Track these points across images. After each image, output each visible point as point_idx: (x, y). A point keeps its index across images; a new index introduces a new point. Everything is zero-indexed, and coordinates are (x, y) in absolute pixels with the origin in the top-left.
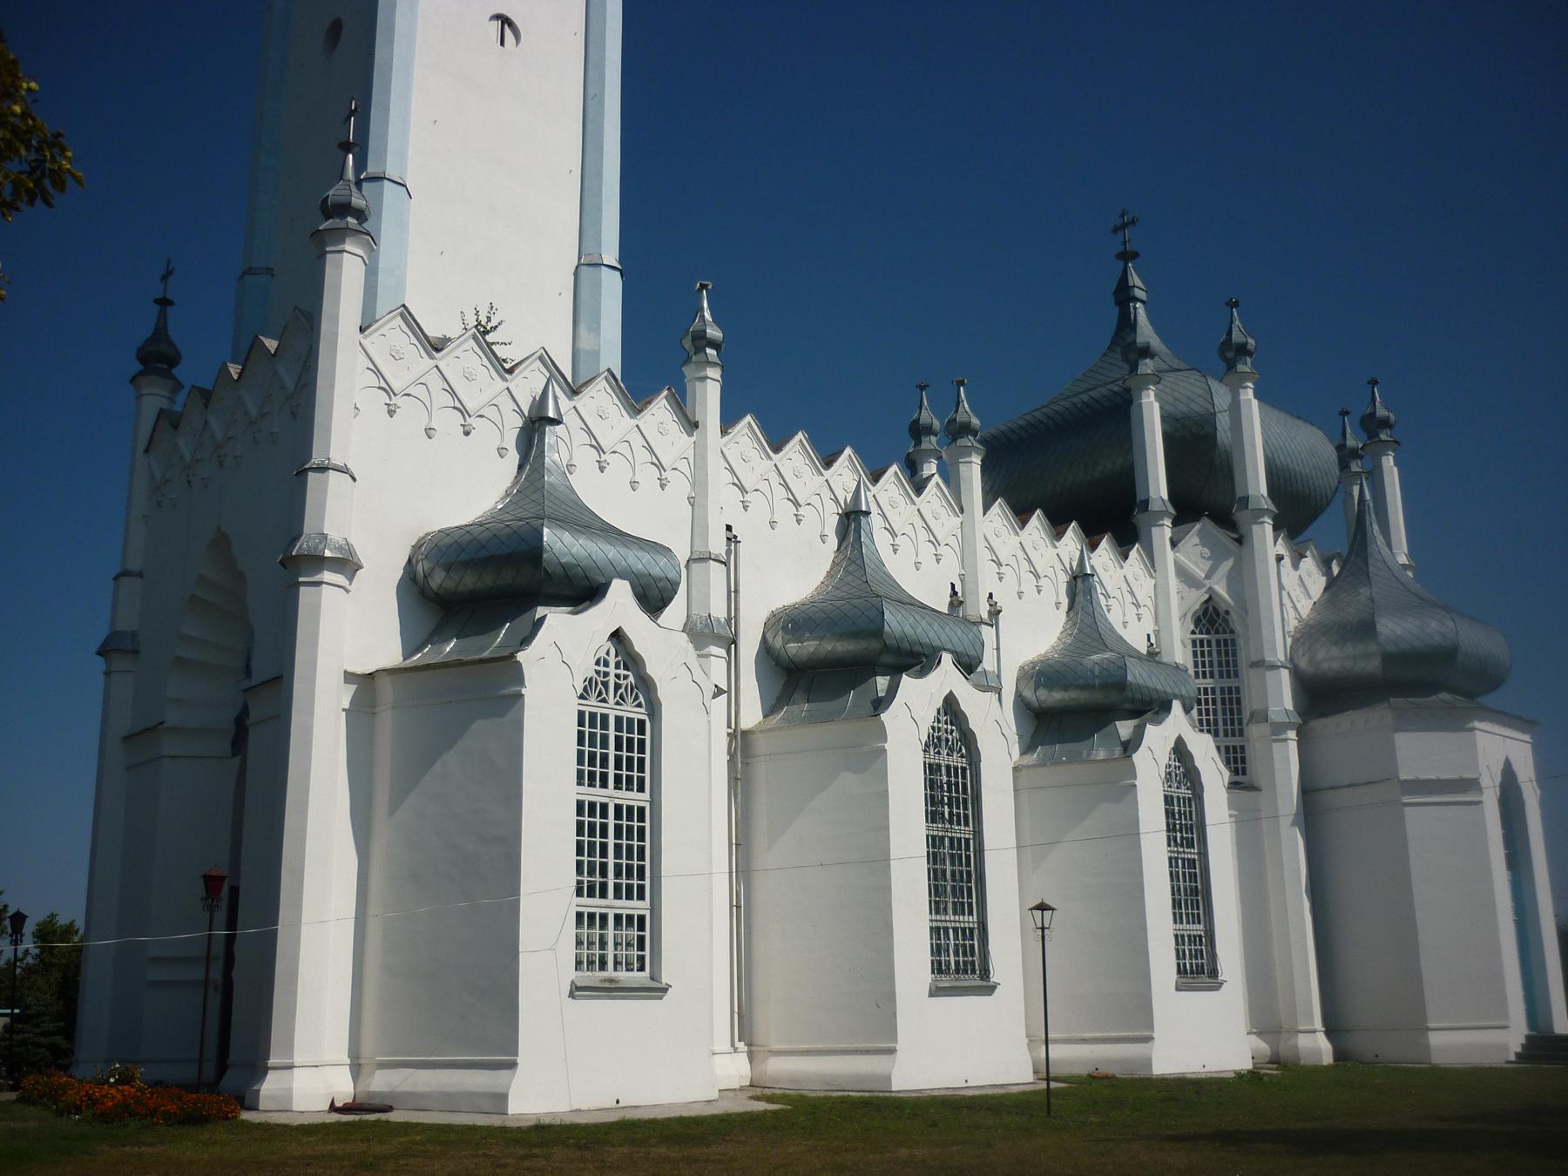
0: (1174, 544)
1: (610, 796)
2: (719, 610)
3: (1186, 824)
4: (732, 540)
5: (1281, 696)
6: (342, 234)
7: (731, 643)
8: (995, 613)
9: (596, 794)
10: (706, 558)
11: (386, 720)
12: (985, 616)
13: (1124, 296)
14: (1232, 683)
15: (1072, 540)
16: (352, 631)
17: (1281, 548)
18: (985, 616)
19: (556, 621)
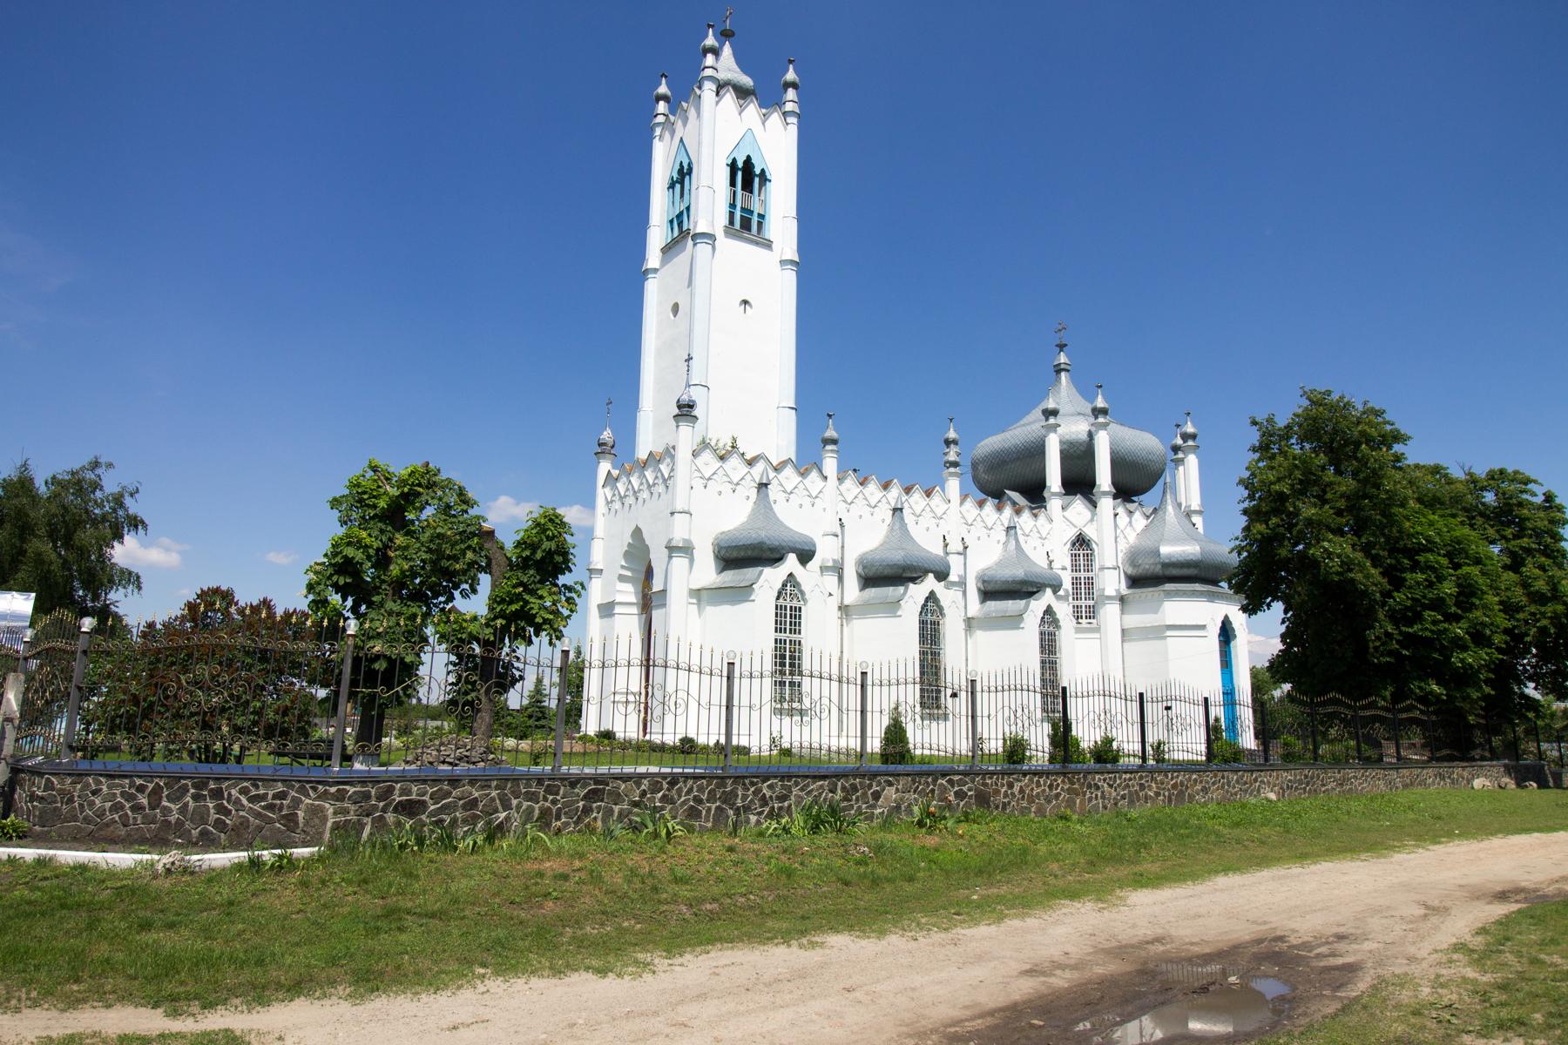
4: (842, 525)
5: (1112, 582)
9: (782, 636)
14: (1090, 574)
15: (1008, 511)
17: (1120, 510)
19: (768, 572)
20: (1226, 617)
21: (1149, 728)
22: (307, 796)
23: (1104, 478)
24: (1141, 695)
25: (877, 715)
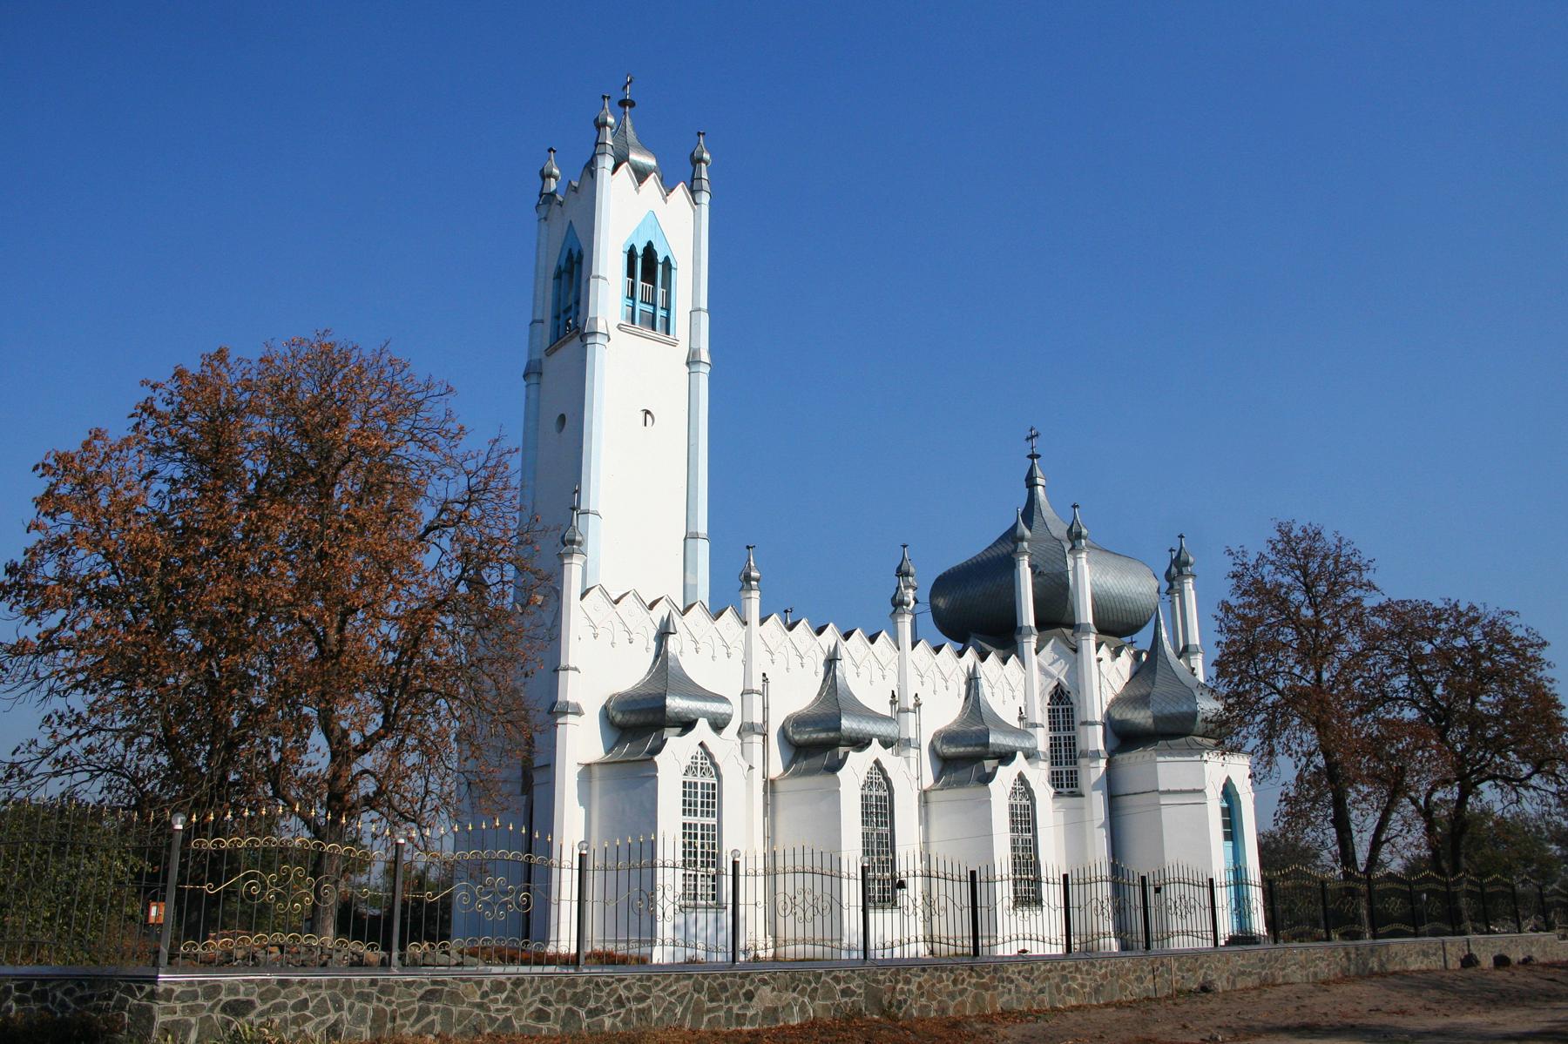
0: (1037, 652)
1: (698, 820)
2: (758, 719)
3: (1024, 819)
5: (1095, 739)
6: (570, 555)
7: (765, 735)
8: (918, 705)
10: (752, 692)
11: (597, 786)
12: (911, 707)
13: (1031, 483)
14: (1071, 734)
15: (970, 656)
16: (581, 742)
17: (1105, 652)
18: (911, 707)
20: (1228, 779)
21: (1074, 914)
22: (134, 996)
23: (1086, 615)
24: (973, 873)
25: (751, 909)
